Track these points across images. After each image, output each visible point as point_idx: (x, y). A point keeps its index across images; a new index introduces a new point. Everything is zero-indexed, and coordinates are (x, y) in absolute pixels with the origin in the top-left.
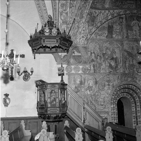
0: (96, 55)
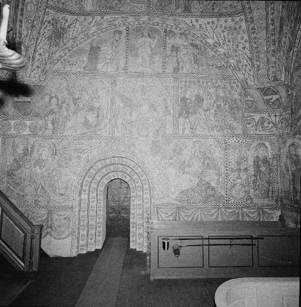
0: (60, 102)
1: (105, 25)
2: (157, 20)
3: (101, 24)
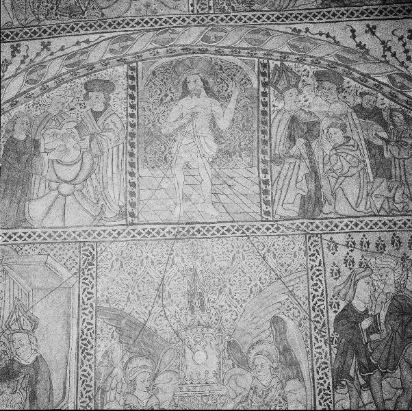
1: (54, 69)
2: (233, 38)
3: (42, 65)
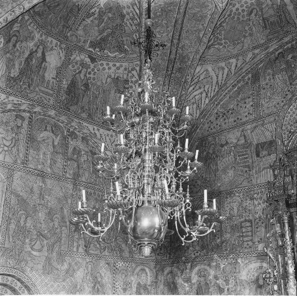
2: (63, 118)
